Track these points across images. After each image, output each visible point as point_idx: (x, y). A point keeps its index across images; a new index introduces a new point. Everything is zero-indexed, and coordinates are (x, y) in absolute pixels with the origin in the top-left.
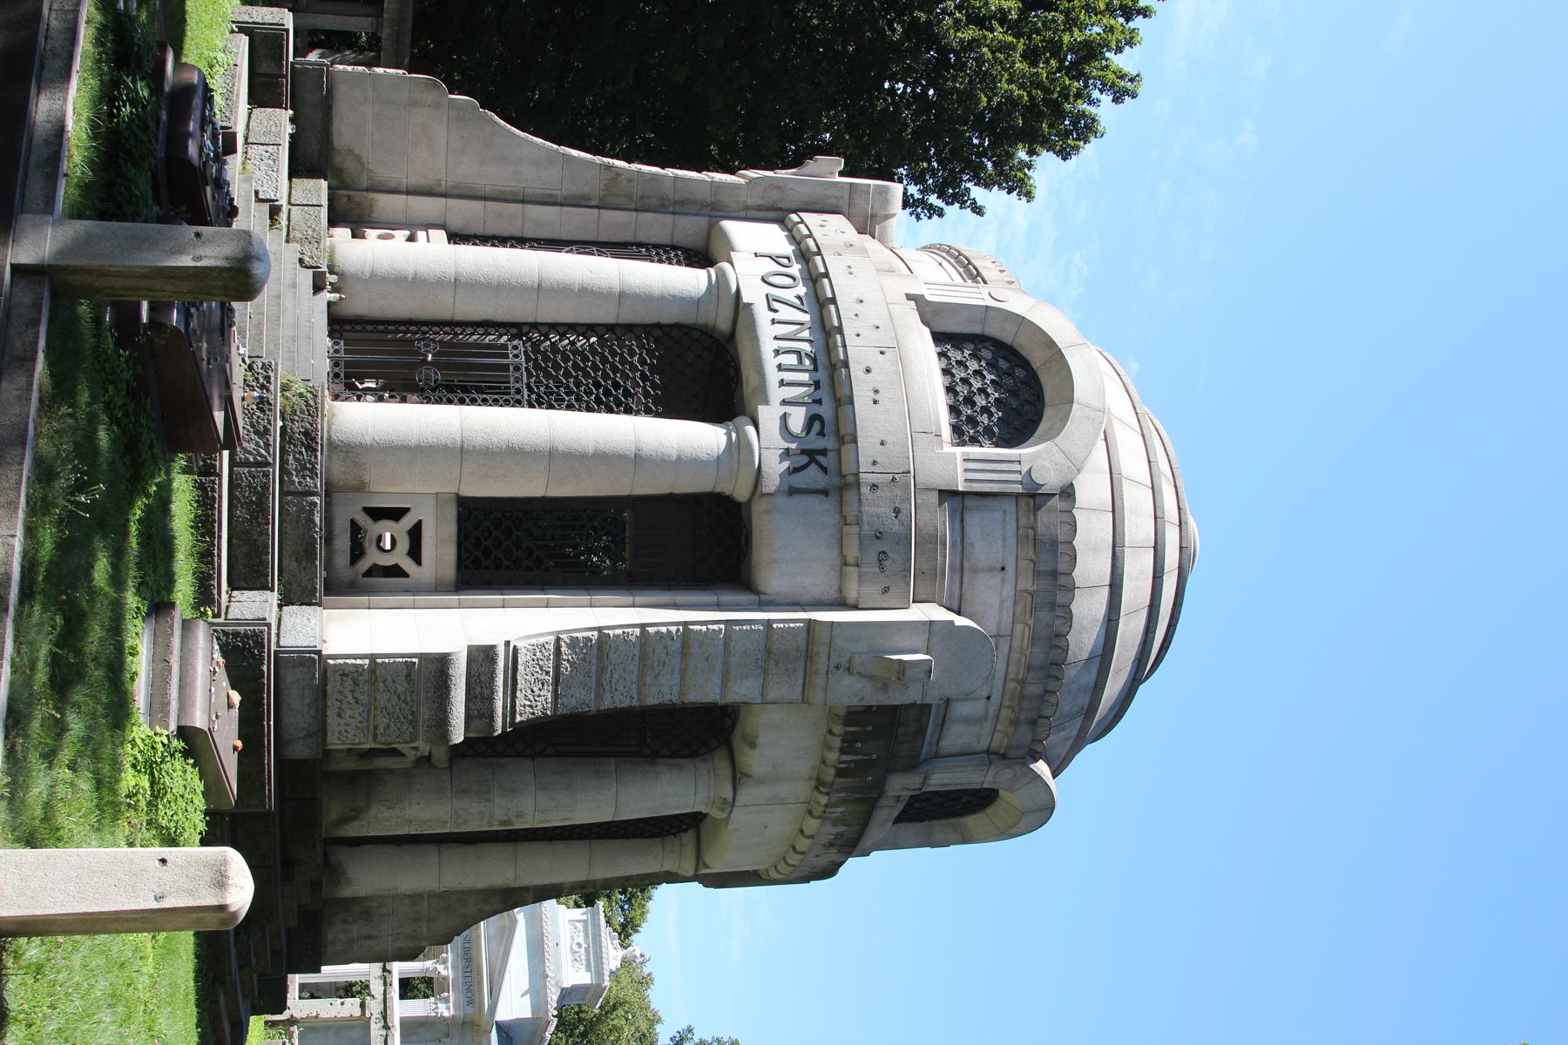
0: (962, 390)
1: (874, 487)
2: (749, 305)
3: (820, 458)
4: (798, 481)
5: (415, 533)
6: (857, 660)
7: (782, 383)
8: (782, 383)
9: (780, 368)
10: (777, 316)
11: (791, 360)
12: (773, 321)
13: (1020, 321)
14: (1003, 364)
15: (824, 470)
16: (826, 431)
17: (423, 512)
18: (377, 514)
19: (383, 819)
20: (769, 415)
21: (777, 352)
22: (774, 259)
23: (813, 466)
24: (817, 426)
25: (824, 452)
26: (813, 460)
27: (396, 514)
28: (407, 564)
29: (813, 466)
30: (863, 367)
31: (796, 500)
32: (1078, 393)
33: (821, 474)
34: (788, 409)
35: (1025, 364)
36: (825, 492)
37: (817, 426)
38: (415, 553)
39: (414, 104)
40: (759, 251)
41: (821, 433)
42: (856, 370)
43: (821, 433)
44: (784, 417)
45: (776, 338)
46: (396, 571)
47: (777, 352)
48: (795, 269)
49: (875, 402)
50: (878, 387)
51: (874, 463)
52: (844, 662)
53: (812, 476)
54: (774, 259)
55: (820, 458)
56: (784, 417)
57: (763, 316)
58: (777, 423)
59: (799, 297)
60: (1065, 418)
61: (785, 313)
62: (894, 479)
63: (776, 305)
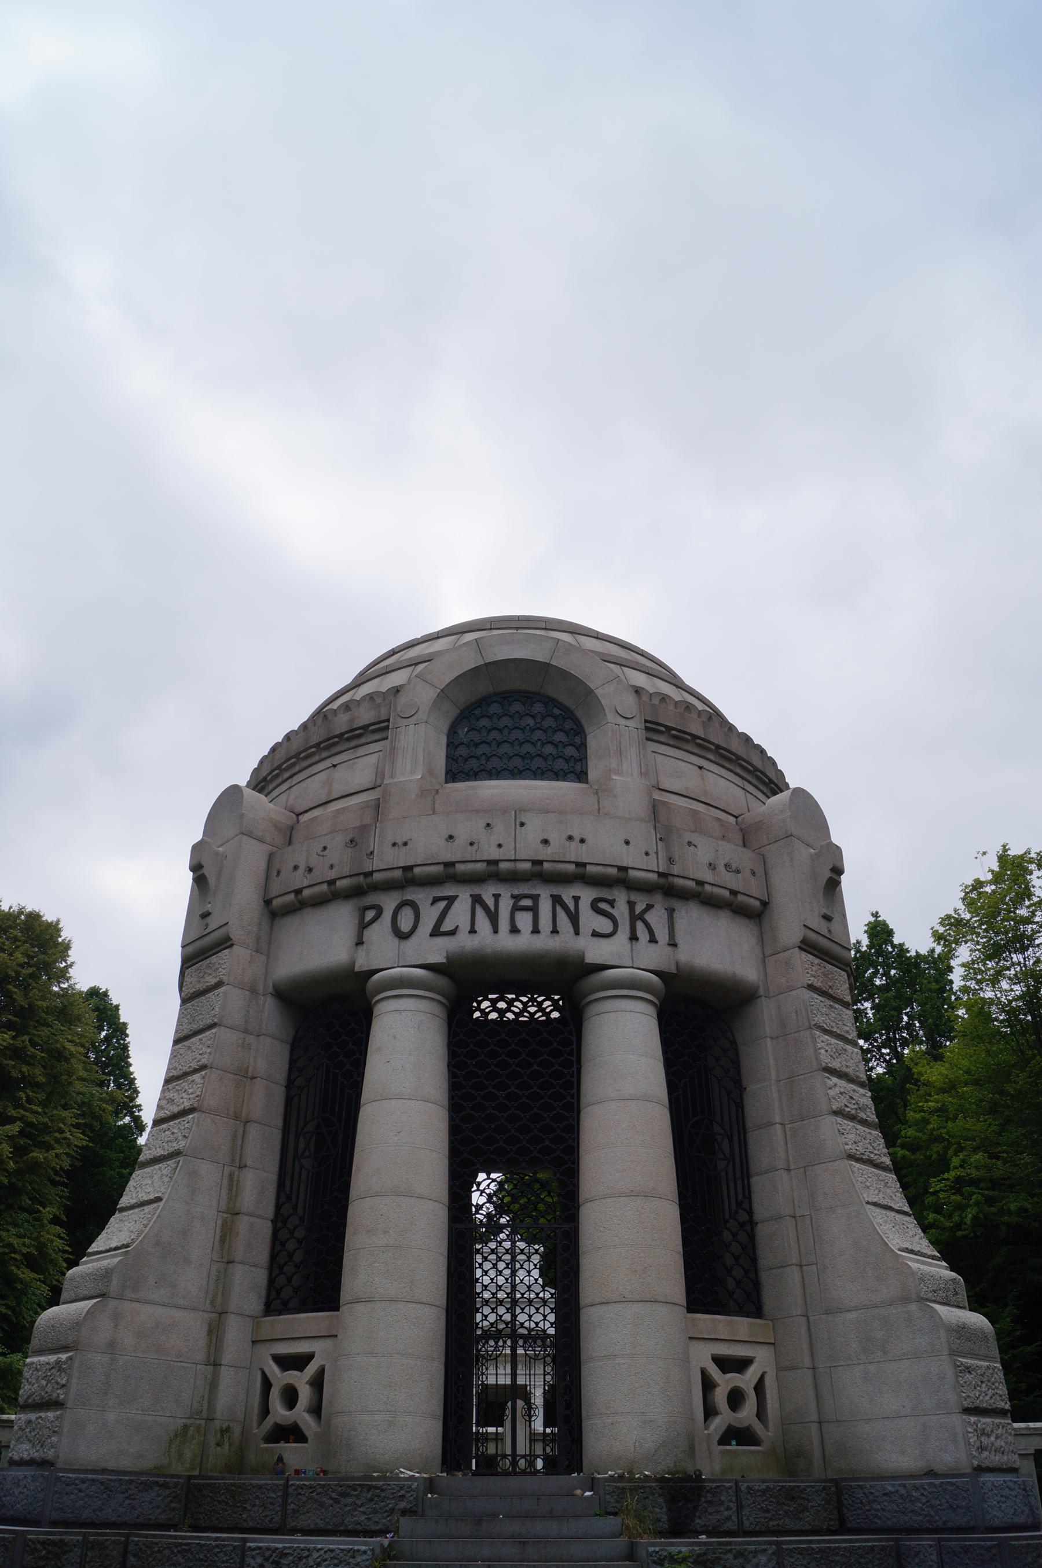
0: (538, 763)
1: (671, 860)
2: (447, 958)
3: (639, 909)
4: (662, 935)
5: (726, 1364)
6: (824, 911)
7: (555, 931)
8: (555, 931)
9: (536, 931)
10: (465, 927)
11: (524, 920)
12: (473, 931)
13: (444, 694)
14: (484, 722)
15: (649, 907)
16: (610, 898)
17: (702, 1356)
18: (710, 1411)
20: (596, 952)
21: (514, 930)
22: (363, 926)
23: (648, 917)
24: (603, 906)
25: (631, 905)
26: (641, 917)
27: (708, 1385)
28: (752, 1374)
29: (648, 917)
30: (541, 846)
31: (680, 939)
32: (540, 656)
33: (653, 911)
35: (485, 701)
36: (671, 911)
37: (603, 906)
38: (740, 1365)
39: (112, 1347)
40: (355, 940)
41: (611, 903)
42: (545, 853)
43: (611, 903)
44: (595, 934)
45: (496, 931)
46: (759, 1388)
47: (514, 930)
48: (389, 902)
49: (582, 841)
50: (565, 836)
51: (647, 854)
52: (823, 922)
53: (657, 918)
54: (363, 926)
55: (639, 909)
56: (595, 934)
57: (464, 942)
58: (604, 942)
59: (436, 900)
60: (565, 675)
62: (661, 839)
63: (447, 926)
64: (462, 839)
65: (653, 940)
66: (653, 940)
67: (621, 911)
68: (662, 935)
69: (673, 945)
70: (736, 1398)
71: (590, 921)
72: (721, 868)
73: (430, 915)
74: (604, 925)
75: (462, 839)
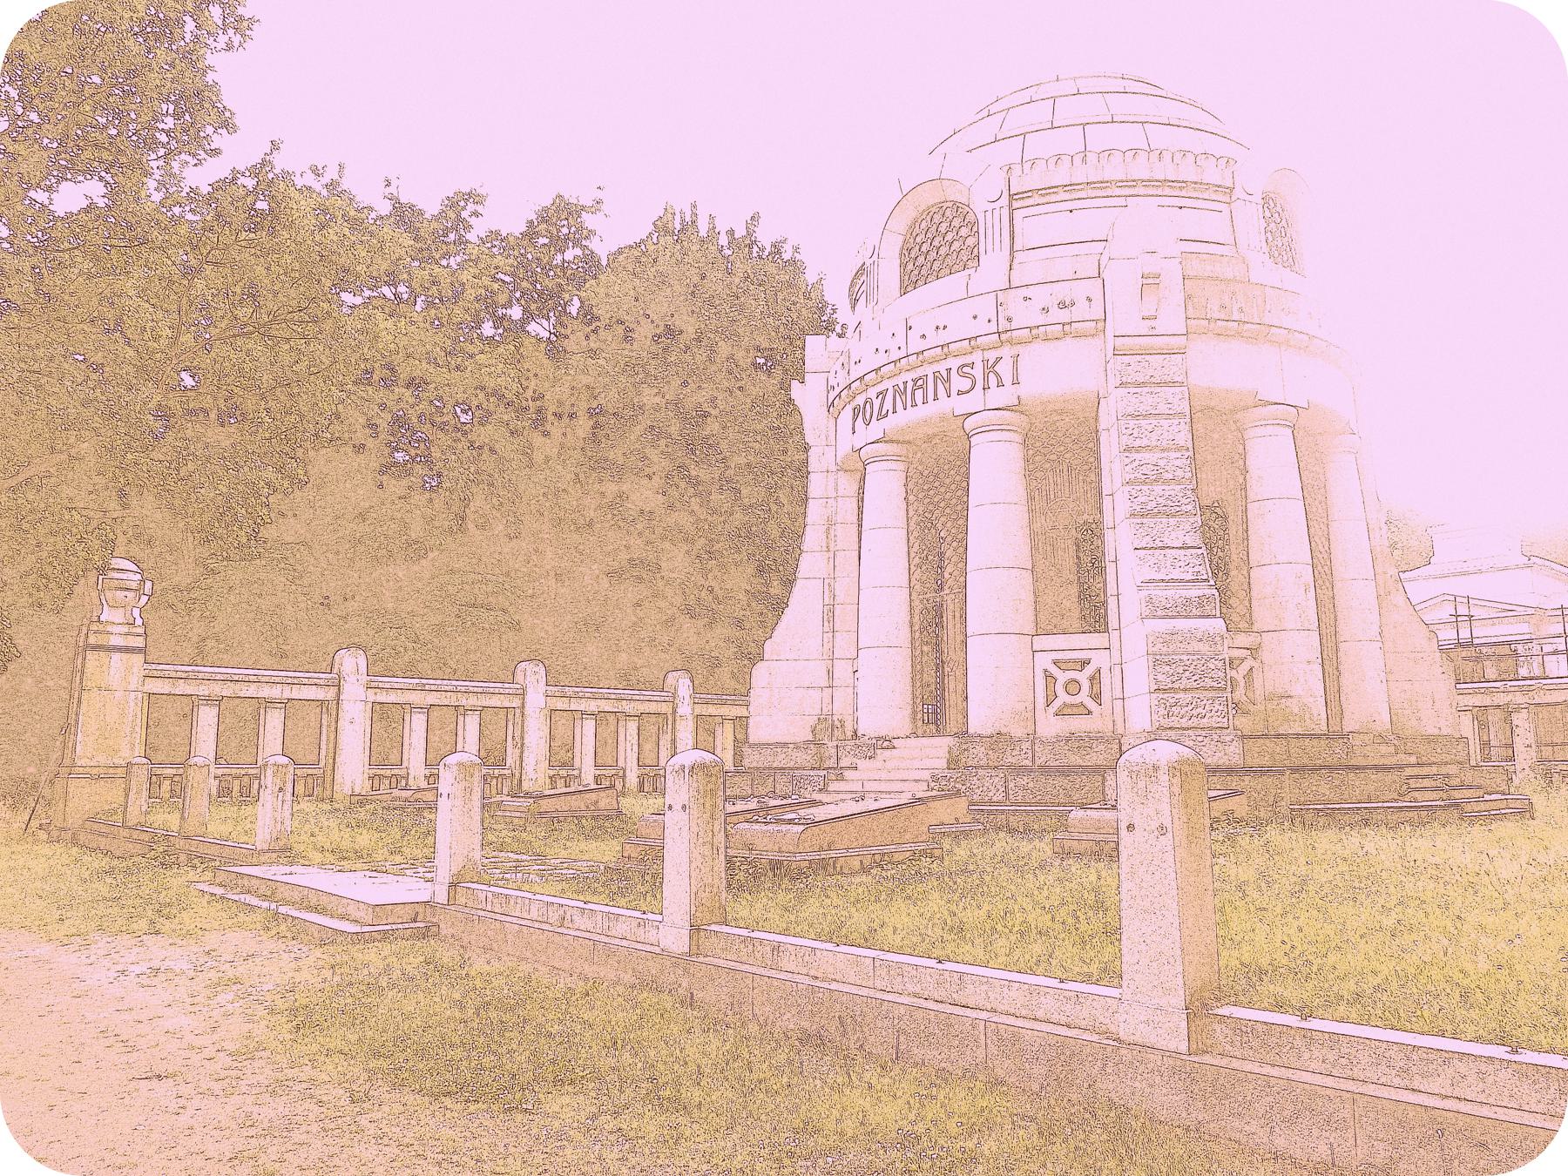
4: (1007, 379)
11: (919, 393)
17: (1044, 661)
19: (1307, 687)
21: (914, 405)
34: (954, 392)
44: (960, 393)
53: (1004, 369)
56: (960, 393)
61: (888, 405)
64: (882, 351)
65: (1000, 384)
66: (1000, 384)
67: (978, 372)
68: (1007, 379)
69: (1016, 382)
70: (1072, 686)
71: (959, 383)
72: (1054, 310)
73: (877, 403)
74: (965, 384)
75: (882, 351)
